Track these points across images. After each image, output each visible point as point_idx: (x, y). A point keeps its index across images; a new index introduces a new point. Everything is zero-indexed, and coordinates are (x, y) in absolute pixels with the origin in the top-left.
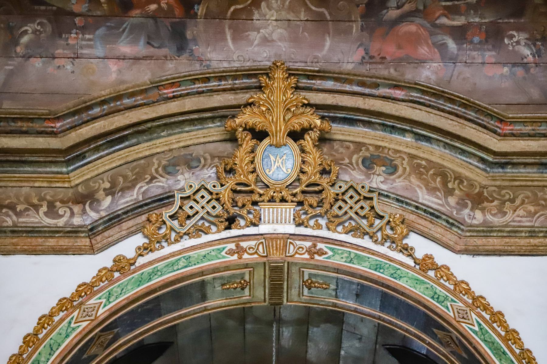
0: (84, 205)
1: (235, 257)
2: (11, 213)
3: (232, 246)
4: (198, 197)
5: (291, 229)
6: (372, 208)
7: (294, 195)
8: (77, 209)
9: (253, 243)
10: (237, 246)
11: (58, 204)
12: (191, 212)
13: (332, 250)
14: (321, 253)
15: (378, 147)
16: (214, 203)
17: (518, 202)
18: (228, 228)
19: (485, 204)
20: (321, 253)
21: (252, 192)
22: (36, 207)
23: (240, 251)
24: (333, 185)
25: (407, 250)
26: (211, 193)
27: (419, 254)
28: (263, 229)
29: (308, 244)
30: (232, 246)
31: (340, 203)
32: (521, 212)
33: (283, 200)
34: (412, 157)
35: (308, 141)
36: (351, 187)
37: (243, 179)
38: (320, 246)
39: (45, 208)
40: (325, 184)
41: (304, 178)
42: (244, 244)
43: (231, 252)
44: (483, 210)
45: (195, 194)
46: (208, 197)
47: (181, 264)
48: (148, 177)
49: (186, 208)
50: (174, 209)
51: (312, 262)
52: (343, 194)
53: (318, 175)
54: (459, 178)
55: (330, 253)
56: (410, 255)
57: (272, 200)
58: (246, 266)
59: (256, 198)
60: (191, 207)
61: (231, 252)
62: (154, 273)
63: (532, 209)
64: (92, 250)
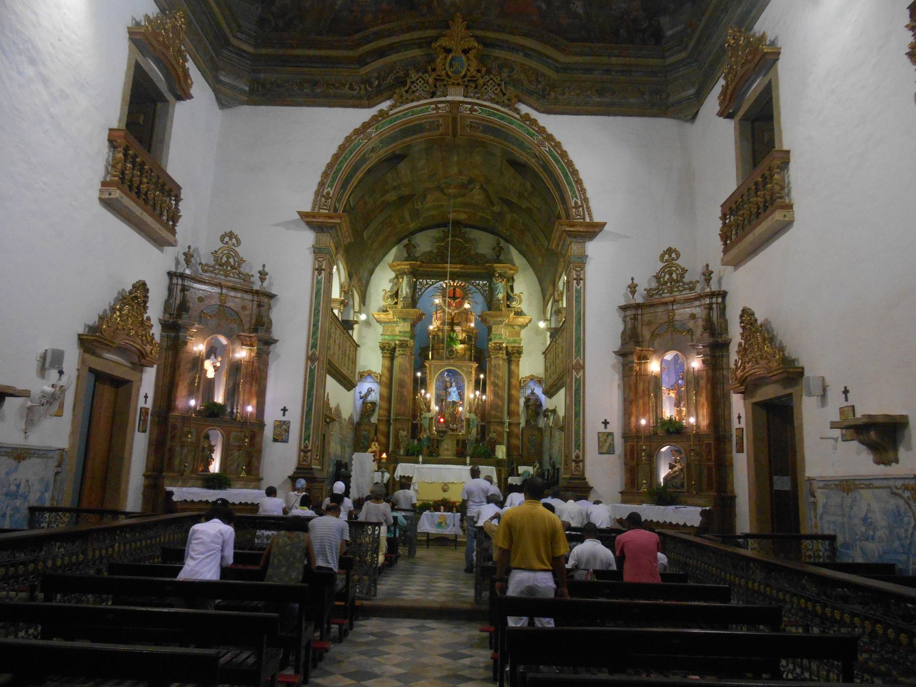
0: (366, 84)
1: (435, 112)
2: (332, 87)
3: (433, 106)
4: (418, 82)
5: (462, 99)
6: (501, 90)
7: (464, 82)
8: (363, 86)
9: (443, 105)
10: (436, 106)
11: (354, 84)
12: (415, 89)
13: (481, 109)
14: (476, 111)
15: (505, 59)
16: (425, 85)
17: (572, 88)
18: (432, 97)
19: (556, 89)
20: (476, 111)
21: (443, 80)
22: (344, 85)
23: (437, 108)
24: (482, 78)
25: (517, 111)
26: (424, 80)
27: (523, 113)
28: (449, 98)
29: (470, 106)
30: (433, 106)
31: (486, 87)
32: (573, 93)
33: (458, 84)
34: (522, 65)
35: (471, 54)
36: (491, 79)
37: (439, 73)
38: (476, 107)
39: (348, 86)
40: (478, 76)
41: (469, 73)
42: (439, 105)
43: (433, 109)
44: (554, 92)
45: (417, 80)
46: (423, 82)
47: (410, 114)
48: (395, 72)
49: (412, 87)
50: (406, 88)
51: (471, 115)
52: (488, 82)
53: (475, 72)
54: (544, 75)
55: (480, 111)
56: (518, 114)
57: (453, 84)
58: (441, 116)
59: (445, 83)
60: (415, 87)
61: (433, 109)
62: (398, 118)
63: (578, 92)
64: (370, 106)
